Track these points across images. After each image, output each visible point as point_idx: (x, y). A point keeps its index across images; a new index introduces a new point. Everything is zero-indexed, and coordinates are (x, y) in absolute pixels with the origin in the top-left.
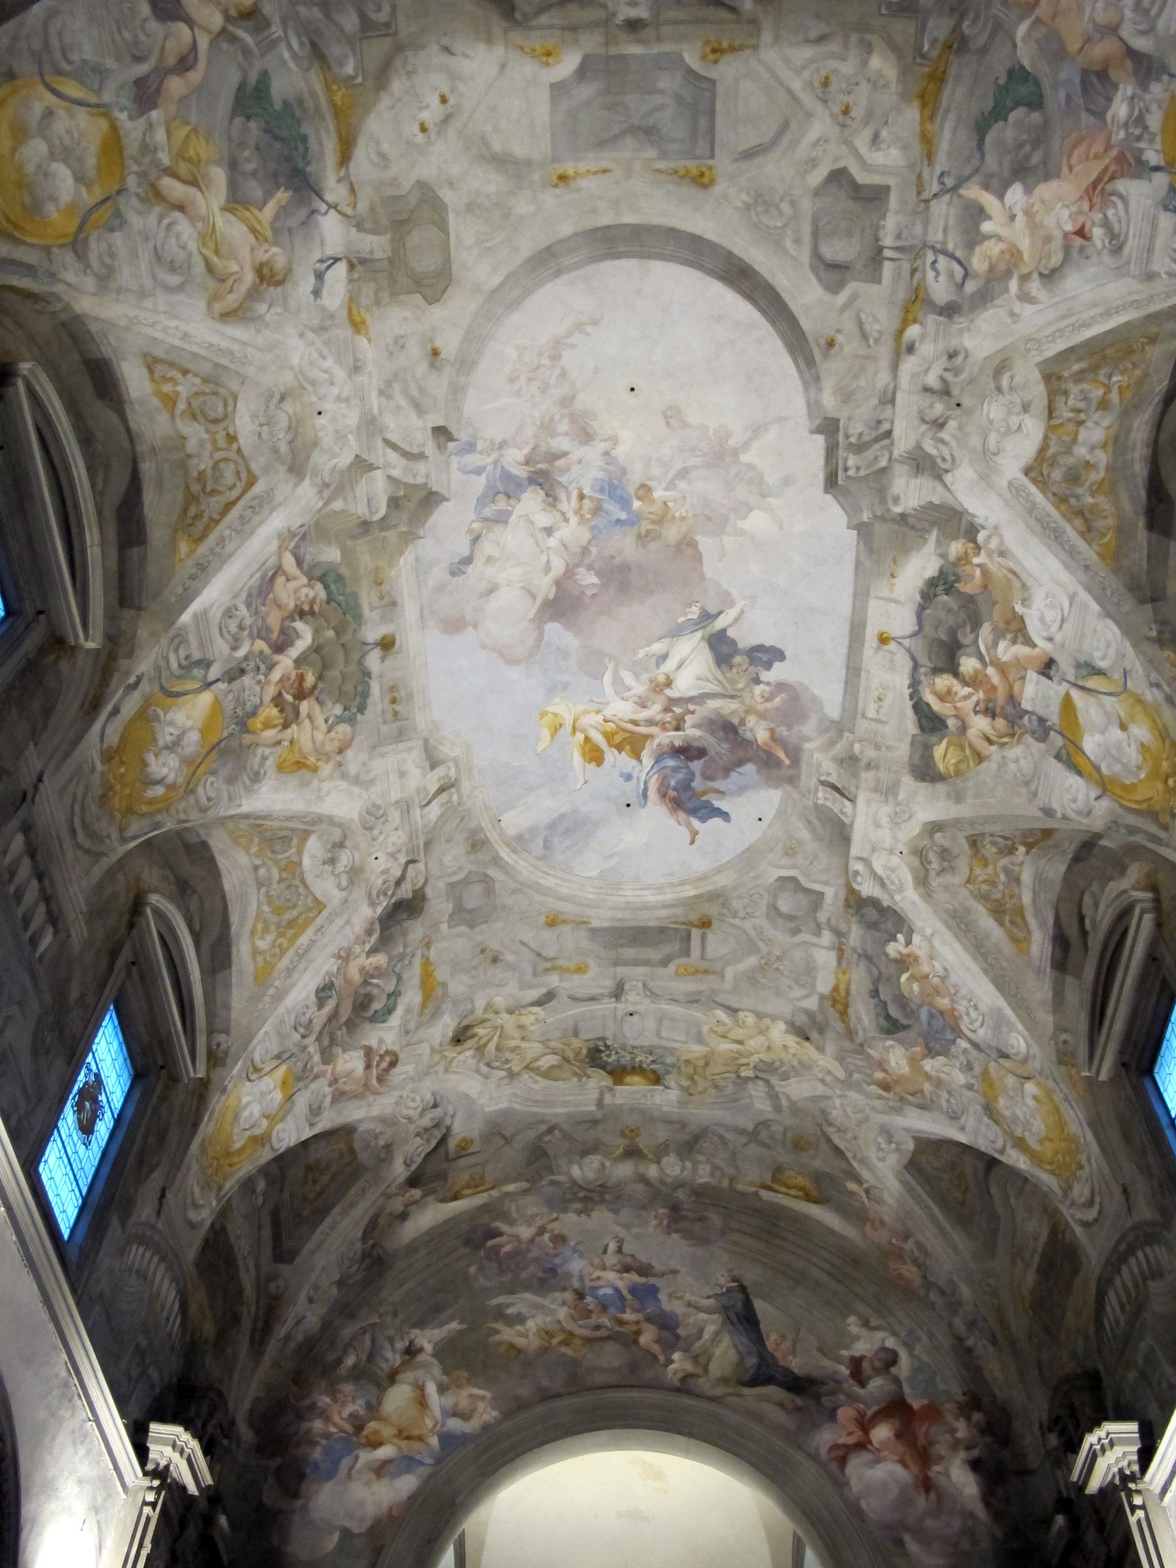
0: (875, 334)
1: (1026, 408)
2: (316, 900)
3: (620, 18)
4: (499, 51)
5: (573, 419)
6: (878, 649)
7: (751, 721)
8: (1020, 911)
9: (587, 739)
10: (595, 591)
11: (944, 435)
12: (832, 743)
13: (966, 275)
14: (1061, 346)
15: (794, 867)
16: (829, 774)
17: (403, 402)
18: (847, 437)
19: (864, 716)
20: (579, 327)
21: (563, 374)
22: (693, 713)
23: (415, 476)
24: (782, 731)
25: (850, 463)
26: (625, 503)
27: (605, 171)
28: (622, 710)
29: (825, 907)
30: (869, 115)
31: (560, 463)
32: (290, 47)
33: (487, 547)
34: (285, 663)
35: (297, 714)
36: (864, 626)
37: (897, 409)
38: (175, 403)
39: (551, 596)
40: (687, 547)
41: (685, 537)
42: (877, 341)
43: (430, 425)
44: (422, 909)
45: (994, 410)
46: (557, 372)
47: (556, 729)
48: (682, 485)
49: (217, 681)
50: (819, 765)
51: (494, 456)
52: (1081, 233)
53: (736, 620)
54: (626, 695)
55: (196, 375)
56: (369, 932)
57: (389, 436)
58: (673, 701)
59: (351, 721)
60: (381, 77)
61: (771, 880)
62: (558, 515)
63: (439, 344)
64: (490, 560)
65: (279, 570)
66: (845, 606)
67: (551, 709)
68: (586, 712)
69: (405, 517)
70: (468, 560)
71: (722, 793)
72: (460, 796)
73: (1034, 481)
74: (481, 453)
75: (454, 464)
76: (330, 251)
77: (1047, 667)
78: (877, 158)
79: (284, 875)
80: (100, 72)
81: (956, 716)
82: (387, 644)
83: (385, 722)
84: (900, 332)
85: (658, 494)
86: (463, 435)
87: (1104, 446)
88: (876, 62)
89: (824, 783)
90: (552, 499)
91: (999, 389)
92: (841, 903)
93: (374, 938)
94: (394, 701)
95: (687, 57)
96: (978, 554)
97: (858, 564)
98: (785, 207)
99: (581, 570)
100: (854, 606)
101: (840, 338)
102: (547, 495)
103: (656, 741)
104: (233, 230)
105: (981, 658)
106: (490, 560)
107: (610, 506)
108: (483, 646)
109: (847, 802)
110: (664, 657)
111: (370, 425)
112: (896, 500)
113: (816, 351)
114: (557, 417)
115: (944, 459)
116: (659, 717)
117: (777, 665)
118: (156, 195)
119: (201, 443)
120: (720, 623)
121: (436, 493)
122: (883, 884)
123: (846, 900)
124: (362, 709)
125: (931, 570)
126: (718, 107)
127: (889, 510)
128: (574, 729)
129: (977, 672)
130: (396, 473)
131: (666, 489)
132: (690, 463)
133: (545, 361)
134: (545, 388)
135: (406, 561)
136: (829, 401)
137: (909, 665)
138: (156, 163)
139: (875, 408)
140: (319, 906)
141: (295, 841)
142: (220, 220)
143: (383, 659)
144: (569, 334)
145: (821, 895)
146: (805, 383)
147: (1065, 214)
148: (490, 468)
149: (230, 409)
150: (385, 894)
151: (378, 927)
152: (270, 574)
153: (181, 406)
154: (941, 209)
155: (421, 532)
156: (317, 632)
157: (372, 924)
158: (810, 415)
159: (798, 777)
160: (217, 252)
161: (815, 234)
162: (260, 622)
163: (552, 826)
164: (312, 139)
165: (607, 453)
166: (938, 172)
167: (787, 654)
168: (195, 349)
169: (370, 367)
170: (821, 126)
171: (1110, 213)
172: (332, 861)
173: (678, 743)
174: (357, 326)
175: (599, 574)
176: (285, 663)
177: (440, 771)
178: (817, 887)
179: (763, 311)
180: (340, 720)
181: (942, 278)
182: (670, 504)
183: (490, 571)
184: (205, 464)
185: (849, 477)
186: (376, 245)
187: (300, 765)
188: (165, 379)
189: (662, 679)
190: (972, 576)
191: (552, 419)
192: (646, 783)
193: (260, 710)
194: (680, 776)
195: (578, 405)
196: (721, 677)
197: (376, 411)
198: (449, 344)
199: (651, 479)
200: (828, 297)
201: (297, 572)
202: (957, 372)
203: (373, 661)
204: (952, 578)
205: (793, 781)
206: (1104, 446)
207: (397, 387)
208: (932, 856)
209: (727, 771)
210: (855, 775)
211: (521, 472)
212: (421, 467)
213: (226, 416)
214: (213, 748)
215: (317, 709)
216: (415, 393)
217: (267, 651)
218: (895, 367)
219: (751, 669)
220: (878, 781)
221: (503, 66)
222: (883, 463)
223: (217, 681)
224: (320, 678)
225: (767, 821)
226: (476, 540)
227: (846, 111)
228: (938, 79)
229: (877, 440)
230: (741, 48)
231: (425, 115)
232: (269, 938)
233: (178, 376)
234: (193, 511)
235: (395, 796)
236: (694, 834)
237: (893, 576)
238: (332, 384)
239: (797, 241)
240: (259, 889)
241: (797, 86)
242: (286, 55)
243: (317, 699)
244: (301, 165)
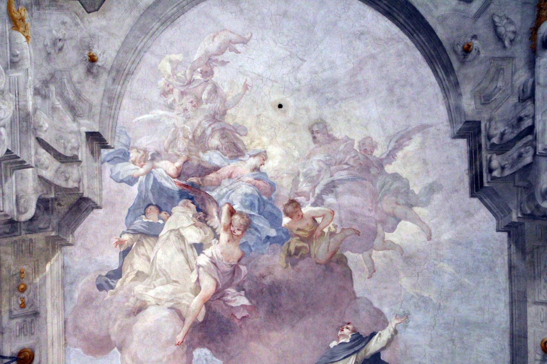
0: (512, 36)
5: (224, 133)
10: (245, 313)
17: (58, 104)
20: (229, 45)
21: (215, 90)
23: (67, 180)
25: (495, 163)
26: (274, 220)
31: (212, 176)
36: (526, 337)
37: (538, 103)
39: (201, 319)
41: (334, 253)
43: (84, 129)
46: (209, 87)
48: (330, 199)
51: (147, 166)
53: (390, 342)
57: (43, 136)
62: (209, 231)
63: (96, 51)
64: (140, 276)
69: (55, 222)
70: (117, 274)
74: (134, 163)
75: (107, 168)
84: (535, 30)
85: (307, 210)
86: (117, 144)
97: (511, 267)
99: (231, 291)
100: (512, 315)
101: (476, 43)
102: (198, 210)
106: (140, 276)
107: (260, 222)
113: (454, 59)
114: (209, 132)
120: (374, 346)
121: (87, 200)
127: (538, 207)
130: (48, 174)
131: (314, 204)
132: (337, 176)
133: (198, 77)
134: (198, 101)
139: (515, 106)
144: (221, 51)
146: (444, 89)
148: (142, 179)
158: (452, 121)
165: (256, 169)
169: (27, 64)
175: (248, 295)
182: (319, 220)
183: (139, 288)
185: (494, 178)
191: (204, 132)
195: (229, 120)
197: (30, 109)
199: (298, 195)
207: (52, 88)
211: (172, 185)
212: (74, 172)
216: (72, 97)
222: (528, 159)
226: (125, 253)
229: (520, 137)
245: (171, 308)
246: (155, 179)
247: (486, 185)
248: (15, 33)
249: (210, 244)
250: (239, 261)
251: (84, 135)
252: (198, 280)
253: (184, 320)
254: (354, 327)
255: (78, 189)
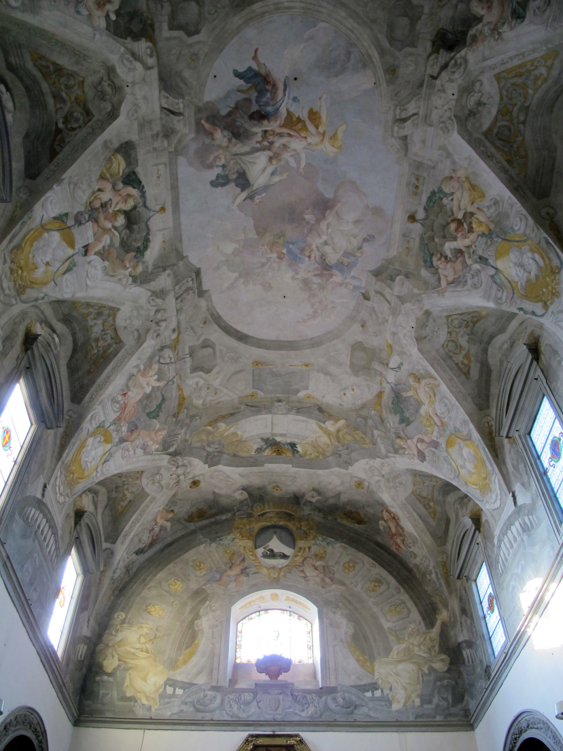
1: (125, 328)
2: (499, 82)
3: (284, 403)
4: (324, 400)
6: (164, 204)
7: (225, 143)
8: (45, 76)
9: (317, 127)
10: (307, 211)
11: (155, 309)
12: (179, 141)
13: (159, 361)
14: (119, 356)
15: (190, 46)
16: (179, 121)
17: (379, 315)
18: (194, 292)
19: (165, 164)
21: (312, 306)
22: (258, 142)
23: (381, 285)
24: (207, 141)
25: (191, 283)
26: (290, 251)
27: (291, 366)
28: (297, 144)
29: (166, 18)
30: (201, 389)
31: (317, 272)
32: (390, 425)
33: (355, 242)
34: (461, 243)
35: (465, 214)
38: (465, 355)
39: (328, 211)
40: (261, 232)
42: (187, 329)
44: (437, 35)
45: (137, 323)
47: (334, 137)
48: (264, 260)
49: (492, 266)
50: (184, 125)
52: (125, 394)
53: (236, 197)
54: (293, 153)
55: (453, 361)
56: (474, 39)
57: (388, 305)
58: (269, 148)
59: (440, 191)
60: (363, 406)
61: (204, 30)
63: (361, 328)
64: (355, 236)
65: (450, 283)
66: (184, 220)
67: (335, 150)
68: (316, 145)
70: (365, 240)
71: (239, 91)
72: (395, 110)
73: (115, 308)
74: (351, 284)
75: (363, 285)
76: (394, 372)
77: (86, 250)
78: (196, 380)
79: (511, 107)
80: (445, 458)
81: (119, 191)
82: (412, 218)
83: (424, 178)
84: (179, 334)
85: (275, 255)
87: (91, 327)
88: (200, 402)
89: (180, 114)
90: (323, 257)
91: (137, 330)
92: (157, 26)
93: (472, 32)
94: (417, 187)
95: (262, 393)
96: (130, 272)
97: (181, 241)
98: (226, 359)
99: (312, 222)
101: (202, 325)
102: (325, 260)
103: (278, 123)
104: (423, 396)
105: (115, 228)
108: (365, 195)
109: (166, 106)
110: (273, 174)
111: (395, 312)
112: (169, 275)
113: (210, 319)
114: (317, 290)
115: (153, 300)
116: (276, 138)
117: (214, 178)
118: (442, 423)
119: (462, 337)
120: (244, 195)
121: (374, 275)
122: (133, 55)
123: (153, 30)
124: (433, 193)
125: (148, 253)
126: (252, 382)
127: (171, 270)
128: (324, 134)
129: (116, 220)
130: (388, 290)
131: (271, 258)
133: (319, 311)
135: (393, 253)
136: (203, 303)
137: (148, 203)
138: (439, 429)
140: (498, 77)
141: (495, 131)
142: (427, 402)
143: (416, 212)
145: (172, 28)
147: (131, 396)
149: (446, 343)
150: (456, 62)
151: (468, 39)
152: (452, 285)
153: (463, 353)
154: (172, 374)
155: (384, 262)
156: (442, 245)
157: (471, 44)
158: (210, 297)
159: (195, 113)
160: (431, 397)
161: (215, 353)
162: (465, 270)
163: (344, 69)
164: (390, 401)
165: (297, 273)
166: (175, 384)
167: (209, 186)
168: (450, 372)
170: (216, 383)
171: (118, 406)
172: (479, 103)
173: (265, 122)
174: (390, 347)
175: (304, 219)
176: (461, 243)
177: (403, 133)
178: (176, 33)
179: (231, 327)
180: (446, 195)
181: (167, 356)
182: (269, 251)
184: (463, 330)
185: (191, 277)
186: (376, 366)
187: (473, 187)
188: (465, 365)
189: (274, 162)
190: (130, 262)
192: (285, 95)
193: (480, 233)
194: (264, 100)
196: (243, 165)
197: (391, 317)
198: (356, 327)
200: (208, 337)
201: (442, 277)
202: (155, 331)
203: (421, 215)
204: (138, 255)
205: (199, 110)
206: (91, 327)
207: (380, 321)
208: (108, 90)
209: (237, 107)
210: (164, 126)
211: (335, 271)
213: (449, 341)
214: (507, 240)
215: (455, 209)
217: (467, 256)
218: (179, 323)
219: (227, 173)
220: (151, 129)
221: (324, 397)
222: (177, 287)
223: (492, 266)
224: (448, 224)
225: (211, 77)
226: (360, 248)
227: (208, 388)
228: (180, 405)
229: (181, 295)
230: (244, 397)
231: (352, 392)
232: (537, 72)
233: (460, 364)
234: (475, 319)
235: (431, 130)
236: (255, 58)
237: (164, 242)
238: (405, 334)
239: (221, 351)
240: (529, 106)
241: (225, 391)
242: (392, 424)
243: (453, 214)
244: (396, 399)
245: (342, 219)
246: (343, 275)
247: (194, 274)
248: (391, 343)
249: (321, 244)
250: (307, 236)
251: (371, 300)
252: (328, 229)
253: (336, 212)
254: (253, 201)
255: (377, 281)
